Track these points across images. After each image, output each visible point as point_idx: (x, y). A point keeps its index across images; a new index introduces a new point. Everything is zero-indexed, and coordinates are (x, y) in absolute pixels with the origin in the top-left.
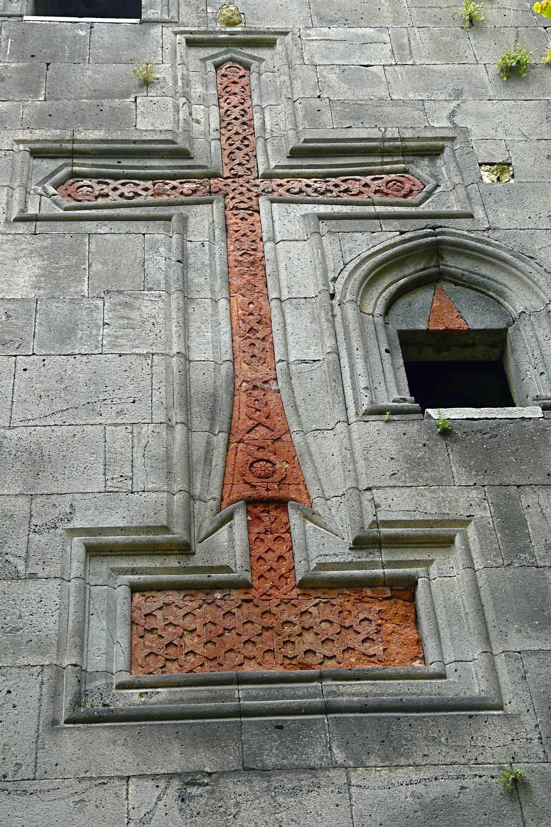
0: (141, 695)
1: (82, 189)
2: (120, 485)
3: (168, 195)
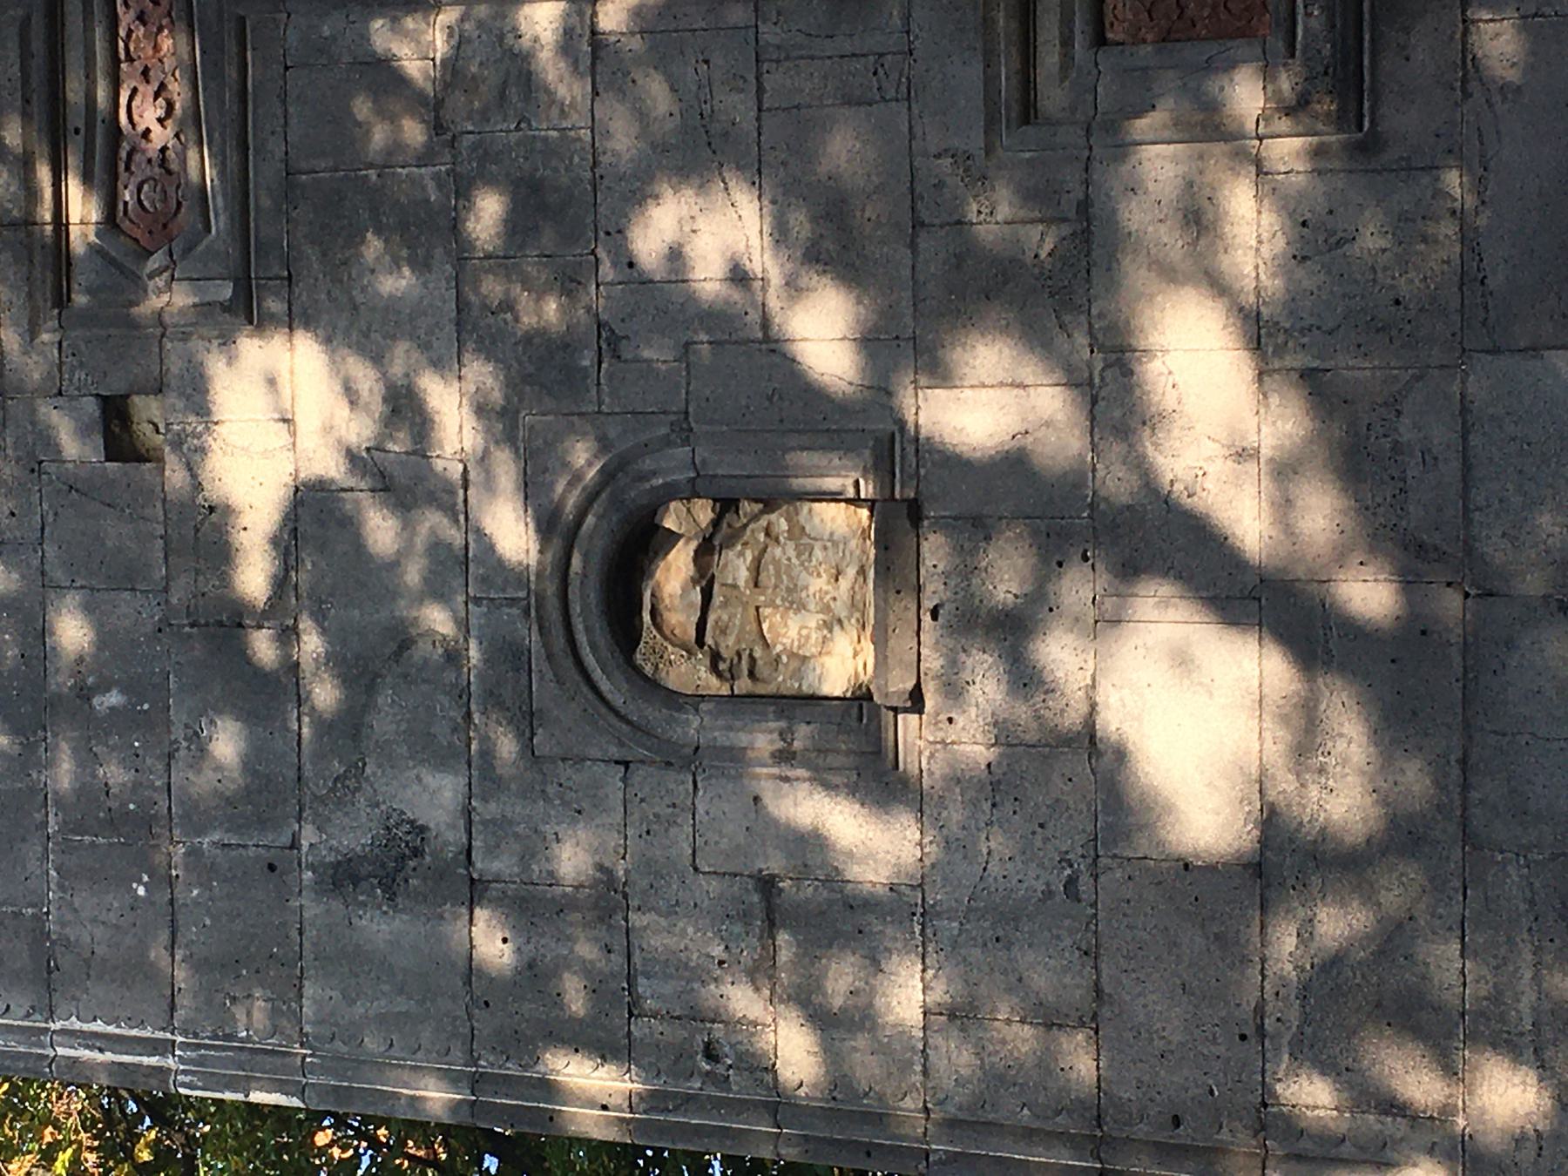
0: (1308, 15)
1: (146, 203)
2: (894, 76)
3: (160, 29)
